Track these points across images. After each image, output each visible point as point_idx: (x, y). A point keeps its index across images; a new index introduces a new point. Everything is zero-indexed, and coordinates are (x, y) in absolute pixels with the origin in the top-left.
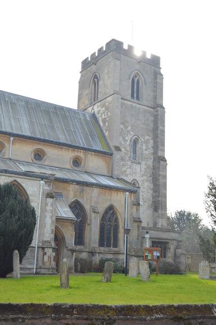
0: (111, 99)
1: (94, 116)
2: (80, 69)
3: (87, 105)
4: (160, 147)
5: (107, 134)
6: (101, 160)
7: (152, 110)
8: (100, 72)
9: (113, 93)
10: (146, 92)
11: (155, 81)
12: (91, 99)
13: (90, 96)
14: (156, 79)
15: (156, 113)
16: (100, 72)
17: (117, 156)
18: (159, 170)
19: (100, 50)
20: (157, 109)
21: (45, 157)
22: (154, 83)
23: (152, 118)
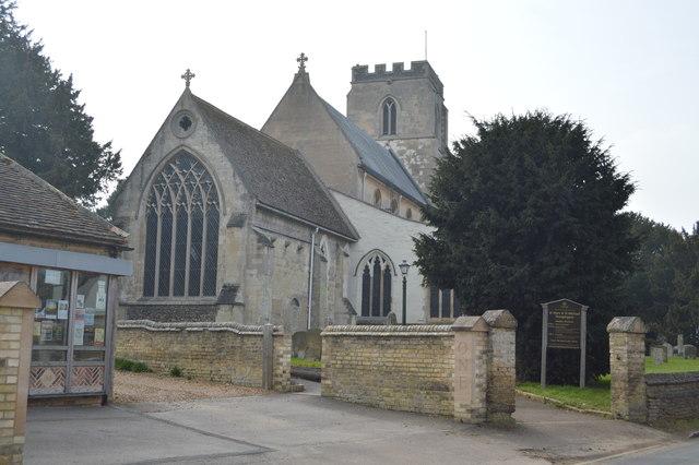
2: (349, 77)
19: (398, 67)
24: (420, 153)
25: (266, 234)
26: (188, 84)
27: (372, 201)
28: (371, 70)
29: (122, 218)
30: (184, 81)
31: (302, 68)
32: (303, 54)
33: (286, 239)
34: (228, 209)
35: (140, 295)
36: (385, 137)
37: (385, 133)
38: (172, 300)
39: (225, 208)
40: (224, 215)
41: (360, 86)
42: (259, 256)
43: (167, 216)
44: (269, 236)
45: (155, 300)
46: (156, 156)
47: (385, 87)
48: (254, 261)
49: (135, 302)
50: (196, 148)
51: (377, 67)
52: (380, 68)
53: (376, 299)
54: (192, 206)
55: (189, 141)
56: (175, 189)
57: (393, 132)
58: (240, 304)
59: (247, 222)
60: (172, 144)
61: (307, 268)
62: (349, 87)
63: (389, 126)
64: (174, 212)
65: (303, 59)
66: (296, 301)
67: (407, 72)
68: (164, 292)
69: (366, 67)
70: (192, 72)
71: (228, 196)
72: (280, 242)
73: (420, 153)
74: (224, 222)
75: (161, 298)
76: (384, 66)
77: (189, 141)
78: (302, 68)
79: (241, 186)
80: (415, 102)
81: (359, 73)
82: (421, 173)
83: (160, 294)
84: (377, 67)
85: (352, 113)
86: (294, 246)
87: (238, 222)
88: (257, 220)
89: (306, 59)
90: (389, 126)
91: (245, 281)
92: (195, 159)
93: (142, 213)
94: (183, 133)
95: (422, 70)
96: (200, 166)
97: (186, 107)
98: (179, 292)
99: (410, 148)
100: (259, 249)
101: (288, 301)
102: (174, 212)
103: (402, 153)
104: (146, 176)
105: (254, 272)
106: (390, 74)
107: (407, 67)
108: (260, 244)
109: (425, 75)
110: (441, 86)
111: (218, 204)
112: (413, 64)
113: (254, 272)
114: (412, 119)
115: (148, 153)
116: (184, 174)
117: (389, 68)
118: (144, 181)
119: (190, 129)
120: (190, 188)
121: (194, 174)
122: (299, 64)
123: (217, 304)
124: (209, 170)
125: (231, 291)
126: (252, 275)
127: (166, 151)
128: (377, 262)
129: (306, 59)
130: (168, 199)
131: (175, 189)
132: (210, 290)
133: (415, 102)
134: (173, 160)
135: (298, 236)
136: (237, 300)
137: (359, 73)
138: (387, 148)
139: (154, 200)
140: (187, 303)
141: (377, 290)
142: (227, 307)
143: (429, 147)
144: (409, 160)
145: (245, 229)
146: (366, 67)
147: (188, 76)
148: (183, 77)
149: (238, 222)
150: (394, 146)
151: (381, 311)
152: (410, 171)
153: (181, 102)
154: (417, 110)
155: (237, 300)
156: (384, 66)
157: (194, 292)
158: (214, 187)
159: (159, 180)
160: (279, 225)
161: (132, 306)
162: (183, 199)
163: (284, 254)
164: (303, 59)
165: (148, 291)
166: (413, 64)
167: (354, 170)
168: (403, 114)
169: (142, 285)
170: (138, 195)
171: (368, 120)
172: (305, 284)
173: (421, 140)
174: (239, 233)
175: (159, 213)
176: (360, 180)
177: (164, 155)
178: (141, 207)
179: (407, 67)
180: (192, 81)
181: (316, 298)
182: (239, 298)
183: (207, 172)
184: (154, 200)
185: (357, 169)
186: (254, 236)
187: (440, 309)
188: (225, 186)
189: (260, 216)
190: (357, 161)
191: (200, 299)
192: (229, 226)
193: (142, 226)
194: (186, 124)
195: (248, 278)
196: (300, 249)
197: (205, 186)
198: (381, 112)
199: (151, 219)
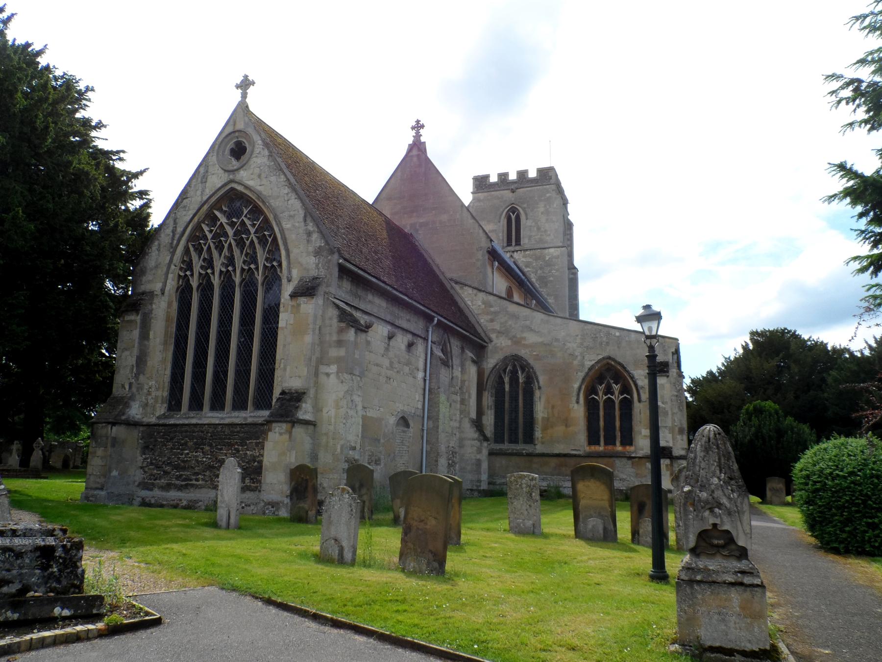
8: (525, 206)
9: (561, 244)
12: (503, 240)
13: (501, 234)
15: (571, 276)
16: (525, 206)
19: (522, 174)
25: (357, 315)
26: (244, 96)
27: (504, 295)
28: (494, 179)
29: (143, 293)
30: (240, 91)
31: (418, 136)
32: (418, 122)
33: (389, 327)
34: (295, 273)
35: (161, 409)
36: (509, 248)
37: (509, 243)
38: (209, 417)
39: (290, 272)
40: (289, 281)
41: (481, 195)
42: (340, 343)
43: (206, 288)
44: (363, 319)
45: (185, 417)
46: (195, 200)
47: (507, 194)
48: (334, 352)
49: (153, 420)
50: (250, 183)
51: (500, 175)
52: (503, 177)
53: (514, 421)
54: (243, 270)
55: (243, 175)
56: (220, 248)
57: (518, 242)
58: (307, 423)
59: (321, 290)
60: (217, 180)
61: (420, 375)
64: (216, 281)
65: (418, 126)
66: (404, 421)
67: (533, 180)
68: (196, 404)
70: (250, 78)
71: (294, 252)
72: (380, 330)
74: (287, 289)
75: (192, 414)
76: (506, 175)
77: (243, 175)
78: (418, 136)
79: (315, 236)
80: (542, 209)
81: (481, 183)
83: (191, 408)
84: (500, 175)
86: (401, 340)
87: (307, 290)
88: (342, 291)
89: (422, 126)
91: (316, 383)
92: (248, 201)
93: (172, 284)
94: (235, 164)
95: (547, 176)
96: (256, 211)
97: (240, 126)
98: (218, 404)
100: (341, 331)
101: (392, 420)
102: (216, 281)
104: (180, 230)
105: (333, 369)
106: (513, 182)
107: (532, 174)
108: (343, 325)
111: (280, 265)
113: (333, 369)
115: (184, 195)
116: (232, 224)
117: (513, 176)
118: (177, 236)
119: (244, 158)
120: (241, 243)
121: (248, 222)
122: (413, 133)
123: (269, 422)
124: (271, 217)
125: (294, 398)
126: (328, 375)
127: (208, 192)
128: (514, 373)
129: (422, 126)
130: (209, 263)
131: (220, 248)
132: (263, 401)
134: (217, 205)
135: (405, 325)
136: (301, 415)
137: (481, 183)
139: (188, 265)
140: (227, 421)
141: (514, 410)
142: (284, 426)
143: (557, 257)
144: (536, 273)
145: (319, 300)
146: (487, 177)
147: (245, 84)
148: (237, 87)
149: (307, 290)
151: (521, 436)
153: (232, 120)
155: (301, 415)
156: (506, 175)
157: (240, 404)
158: (275, 239)
159: (197, 237)
160: (376, 304)
161: (148, 425)
162: (231, 261)
163: (387, 349)
164: (418, 126)
165: (174, 403)
166: (541, 171)
167: (481, 256)
168: (529, 223)
169: (166, 394)
170: (168, 258)
172: (418, 397)
173: (552, 250)
174: (308, 306)
175: (194, 283)
176: (489, 270)
177: (205, 198)
178: (170, 276)
179: (532, 174)
180: (251, 91)
181: (433, 417)
182: (305, 412)
183: (266, 220)
184: (189, 266)
185: (487, 256)
186: (333, 313)
187: (602, 433)
188: (291, 237)
189: (347, 285)
190: (485, 244)
191: (251, 415)
192: (294, 295)
193: (170, 304)
194: (239, 151)
195: (323, 379)
196: (410, 345)
197: (263, 241)
198: (504, 222)
199: (184, 292)
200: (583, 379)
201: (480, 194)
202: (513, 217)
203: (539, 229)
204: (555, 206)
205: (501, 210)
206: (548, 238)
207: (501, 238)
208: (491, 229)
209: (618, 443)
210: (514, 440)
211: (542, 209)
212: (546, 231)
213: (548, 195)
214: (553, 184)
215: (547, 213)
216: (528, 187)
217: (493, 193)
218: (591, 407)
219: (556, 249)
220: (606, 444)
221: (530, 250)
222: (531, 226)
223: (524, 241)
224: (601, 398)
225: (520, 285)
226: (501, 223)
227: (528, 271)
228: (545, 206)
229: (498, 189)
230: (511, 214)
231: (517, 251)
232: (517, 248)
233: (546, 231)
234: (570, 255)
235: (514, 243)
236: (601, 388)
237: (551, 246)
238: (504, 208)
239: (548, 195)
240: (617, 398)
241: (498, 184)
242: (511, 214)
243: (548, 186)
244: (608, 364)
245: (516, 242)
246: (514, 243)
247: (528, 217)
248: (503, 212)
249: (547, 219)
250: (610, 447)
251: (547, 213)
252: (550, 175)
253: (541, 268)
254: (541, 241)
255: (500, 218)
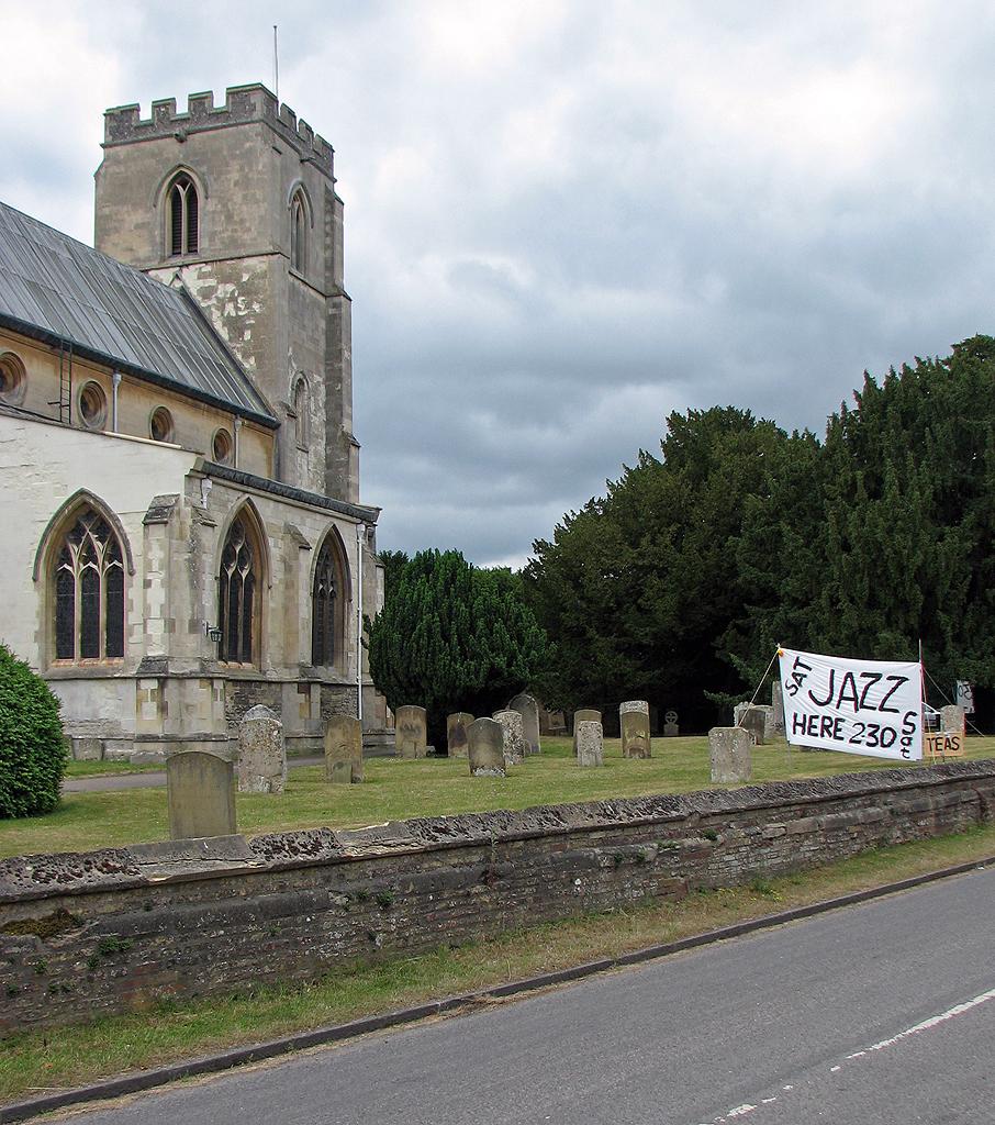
0: (264, 267)
1: (184, 294)
2: (99, 134)
3: (149, 259)
4: (346, 408)
5: (249, 365)
6: (258, 442)
7: (322, 299)
8: (204, 169)
9: (270, 249)
10: (317, 255)
11: (328, 219)
12: (163, 244)
14: (333, 213)
15: (331, 311)
17: (289, 431)
18: (347, 473)
19: (199, 101)
20: (336, 300)
21: (171, 432)
22: (326, 224)
23: (323, 324)
24: (247, 291)
28: (146, 114)
36: (178, 260)
41: (121, 151)
51: (156, 106)
52: (163, 107)
62: (100, 154)
63: (183, 236)
69: (135, 109)
73: (247, 291)
76: (169, 104)
82: (247, 335)
84: (156, 106)
85: (106, 211)
90: (183, 236)
99: (225, 280)
103: (207, 293)
107: (220, 102)
109: (257, 115)
110: (320, 156)
112: (233, 93)
114: (229, 217)
117: (182, 108)
133: (235, 176)
138: (178, 284)
143: (264, 275)
144: (222, 308)
146: (135, 109)
150: (192, 280)
152: (224, 334)
154: (238, 198)
156: (169, 104)
166: (233, 93)
171: (137, 227)
179: (220, 102)
200: (45, 536)
201: (118, 148)
202: (183, 193)
203: (229, 217)
204: (260, 167)
205: (160, 180)
206: (245, 237)
207: (158, 239)
208: (140, 221)
209: (102, 653)
210: (90, 651)
211: (235, 176)
212: (242, 221)
213: (247, 145)
214: (257, 122)
215: (245, 183)
216: (211, 129)
217: (143, 145)
218: (62, 582)
219: (260, 258)
220: (84, 656)
221: (212, 261)
222: (214, 212)
223: (203, 243)
224: (76, 569)
225: (54, 346)
226: (159, 206)
227: (209, 307)
228: (242, 169)
229: (154, 135)
230: (179, 187)
231: (187, 266)
232: (190, 259)
233: (242, 221)
234: (333, 264)
235: (184, 249)
236: (75, 550)
237: (250, 252)
238: (164, 175)
239: (247, 145)
240: (101, 568)
241: (152, 125)
242: (179, 187)
243: (247, 126)
244: (85, 503)
245: (189, 246)
246: (184, 249)
247: (209, 193)
248: (163, 182)
249: (245, 197)
250: (87, 661)
251: (245, 183)
252: (252, 102)
253: (233, 299)
254: (234, 242)
255: (156, 197)
